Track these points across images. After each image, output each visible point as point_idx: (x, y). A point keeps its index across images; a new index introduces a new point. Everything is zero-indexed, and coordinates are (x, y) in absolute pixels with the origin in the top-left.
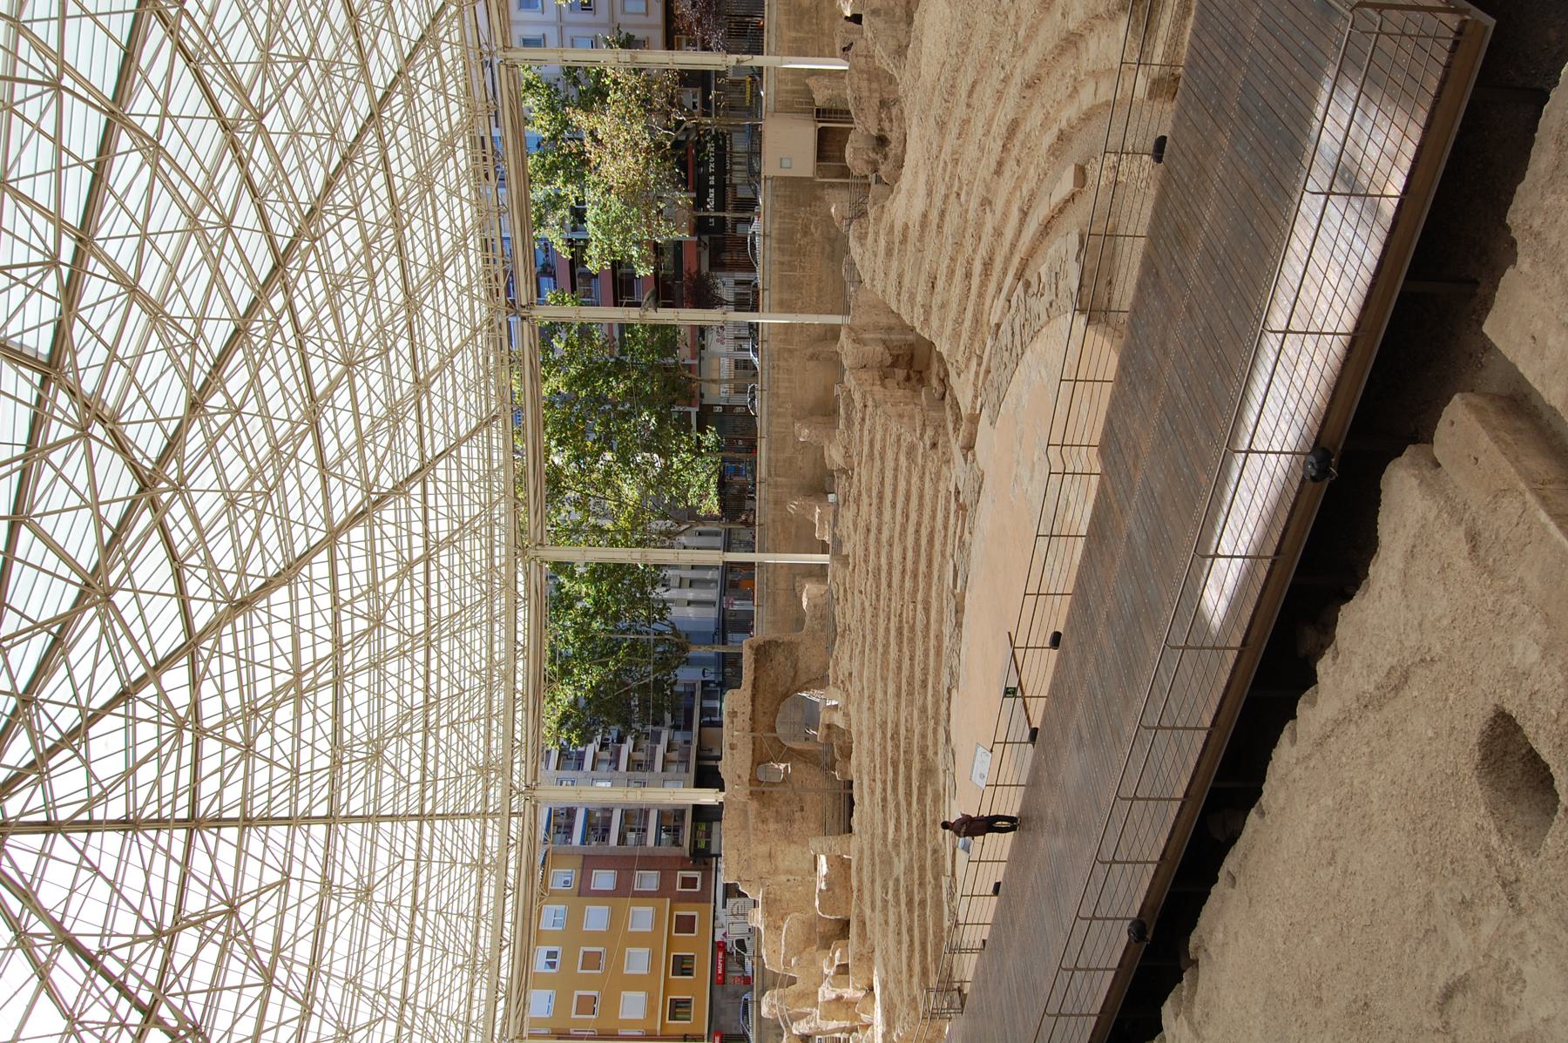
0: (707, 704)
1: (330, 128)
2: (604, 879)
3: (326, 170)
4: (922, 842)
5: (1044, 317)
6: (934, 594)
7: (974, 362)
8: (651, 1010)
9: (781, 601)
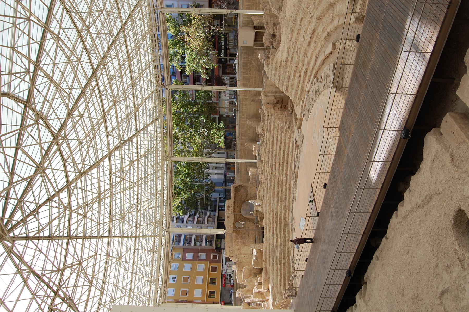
0: (220, 204)
1: (109, 32)
2: (190, 256)
3: (108, 44)
4: (284, 246)
5: (322, 89)
6: (288, 172)
7: (301, 102)
8: (203, 295)
9: (243, 174)
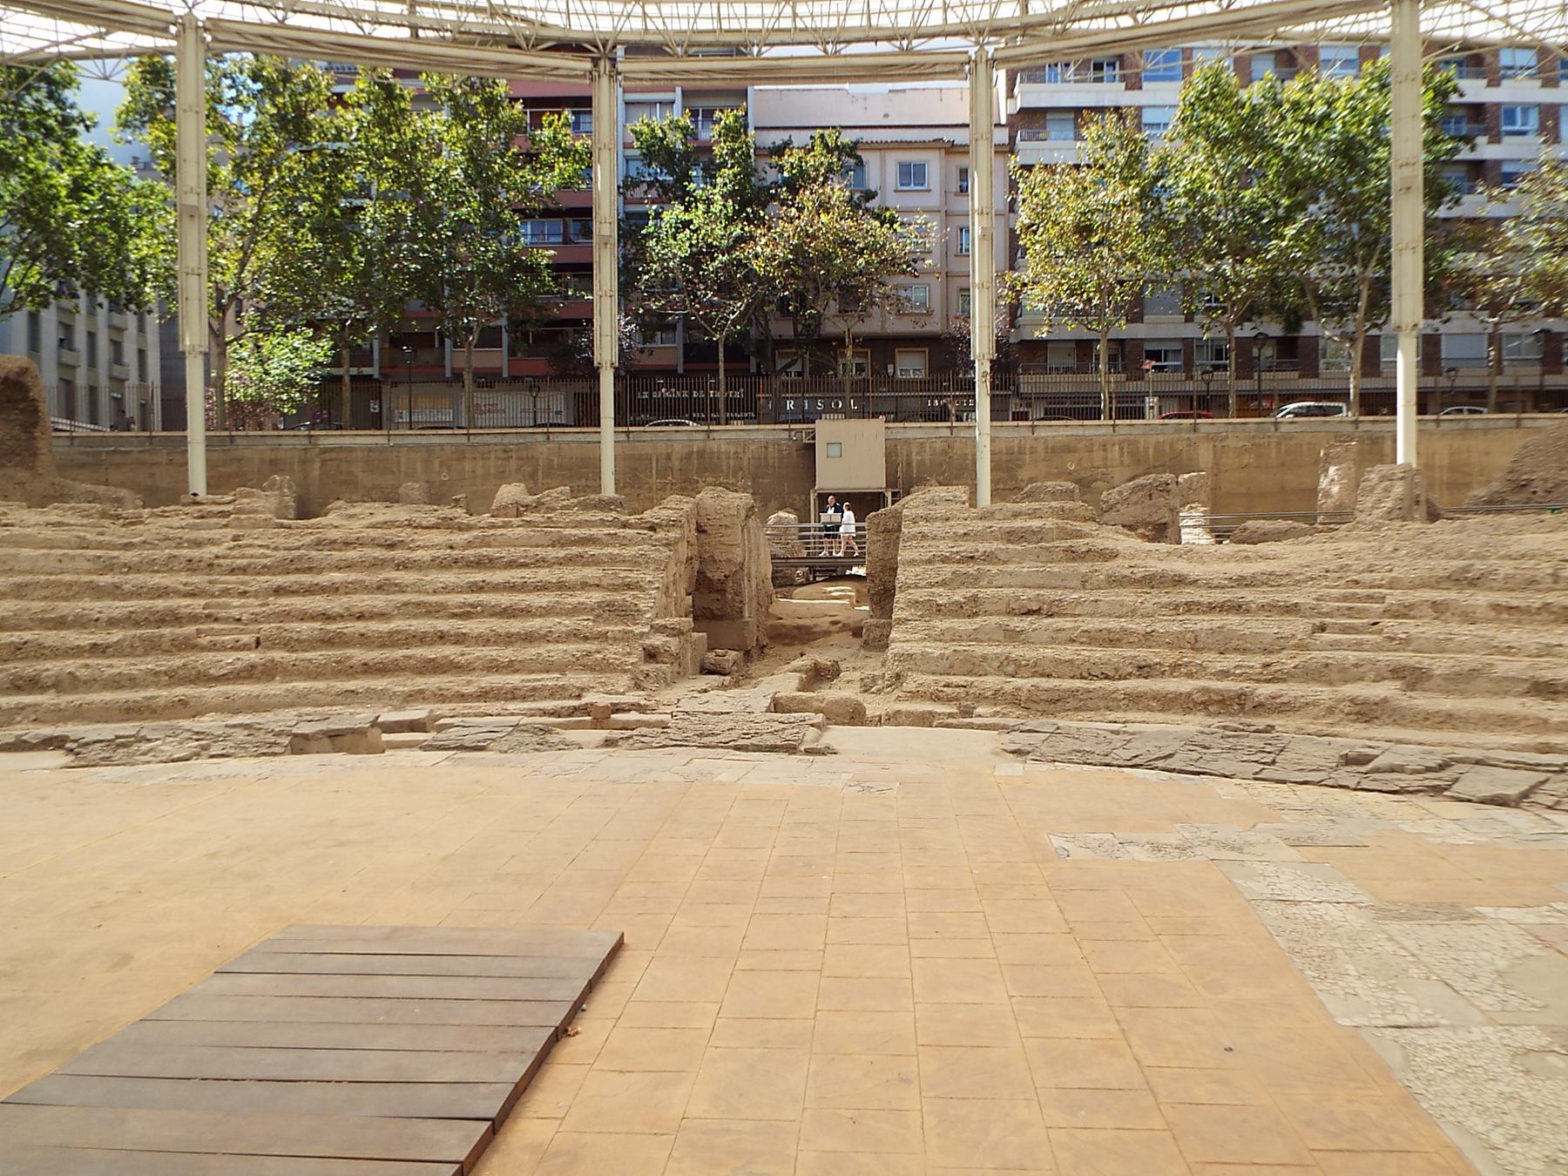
6: (301, 685)
